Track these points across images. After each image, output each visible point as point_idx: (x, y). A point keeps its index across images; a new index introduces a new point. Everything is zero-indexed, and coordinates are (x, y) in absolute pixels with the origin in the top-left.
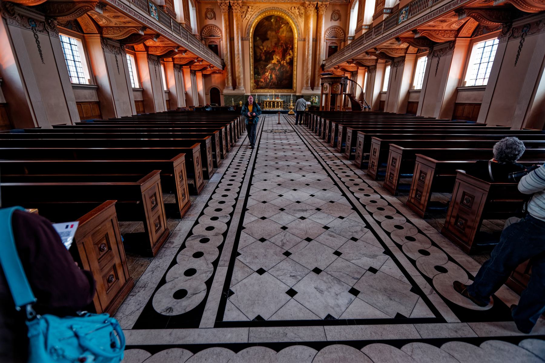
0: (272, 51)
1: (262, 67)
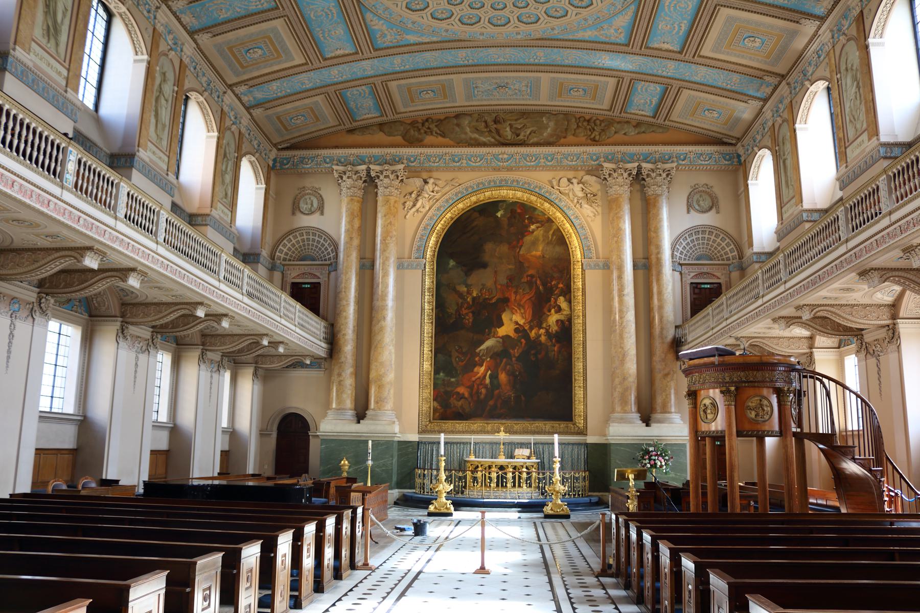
0: (498, 300)
1: (464, 350)
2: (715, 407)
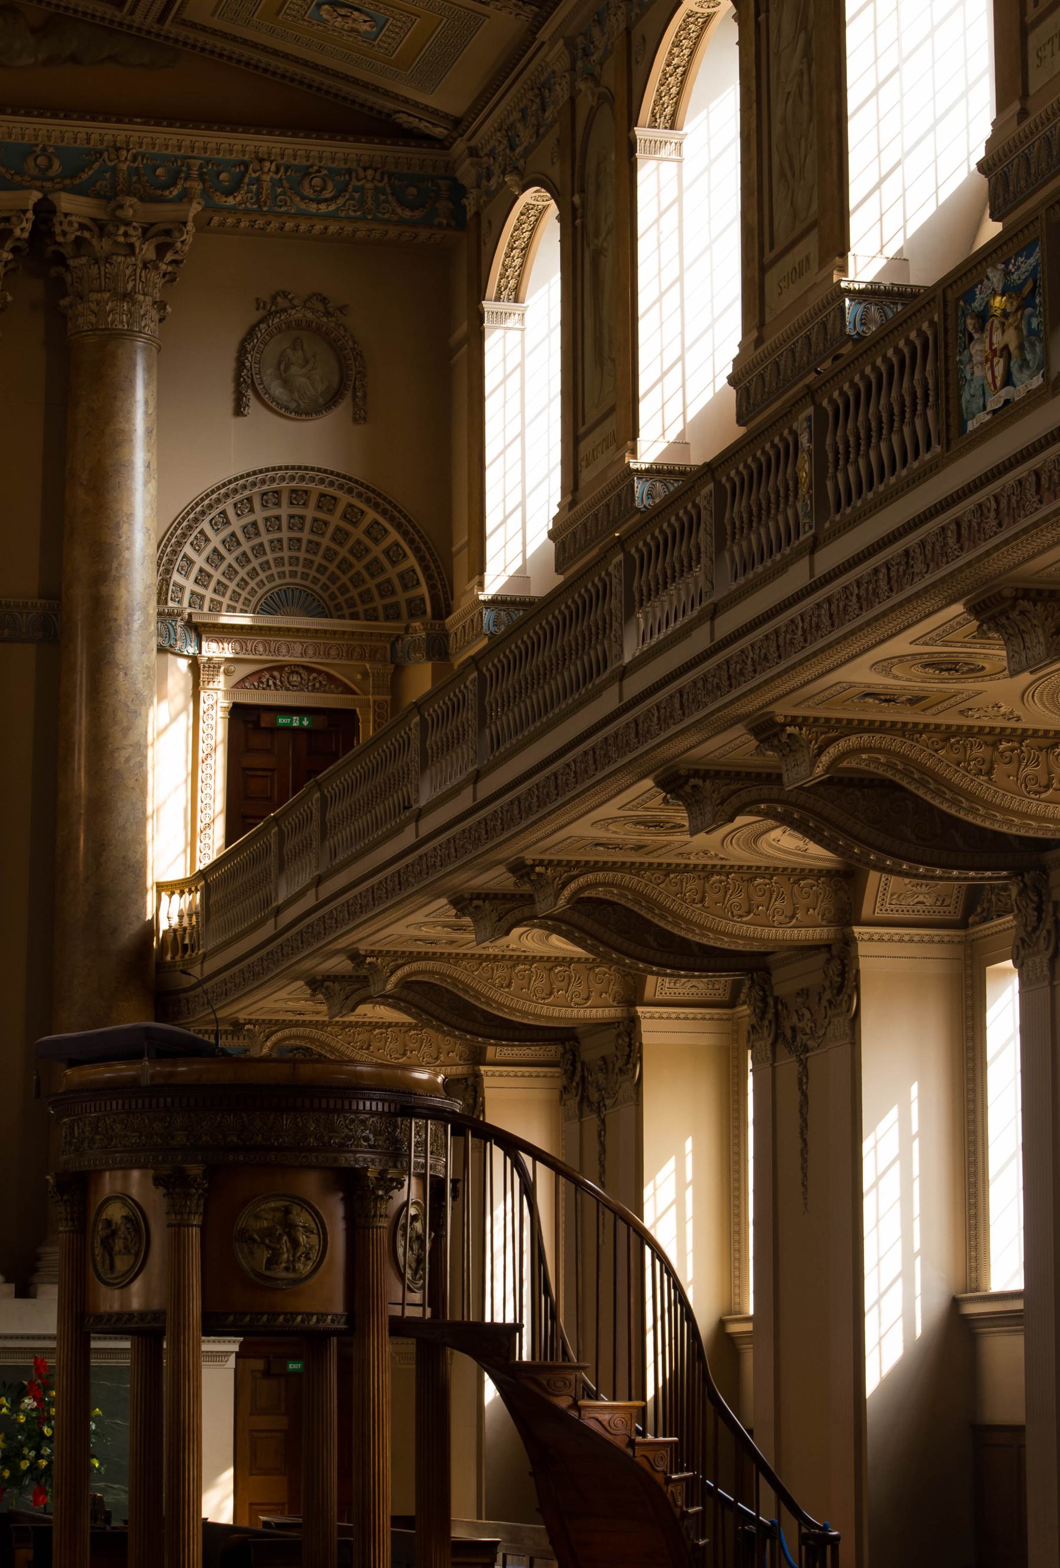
2: (138, 1231)
